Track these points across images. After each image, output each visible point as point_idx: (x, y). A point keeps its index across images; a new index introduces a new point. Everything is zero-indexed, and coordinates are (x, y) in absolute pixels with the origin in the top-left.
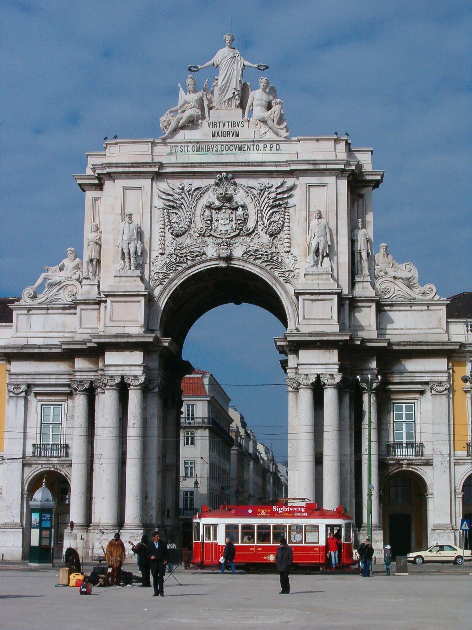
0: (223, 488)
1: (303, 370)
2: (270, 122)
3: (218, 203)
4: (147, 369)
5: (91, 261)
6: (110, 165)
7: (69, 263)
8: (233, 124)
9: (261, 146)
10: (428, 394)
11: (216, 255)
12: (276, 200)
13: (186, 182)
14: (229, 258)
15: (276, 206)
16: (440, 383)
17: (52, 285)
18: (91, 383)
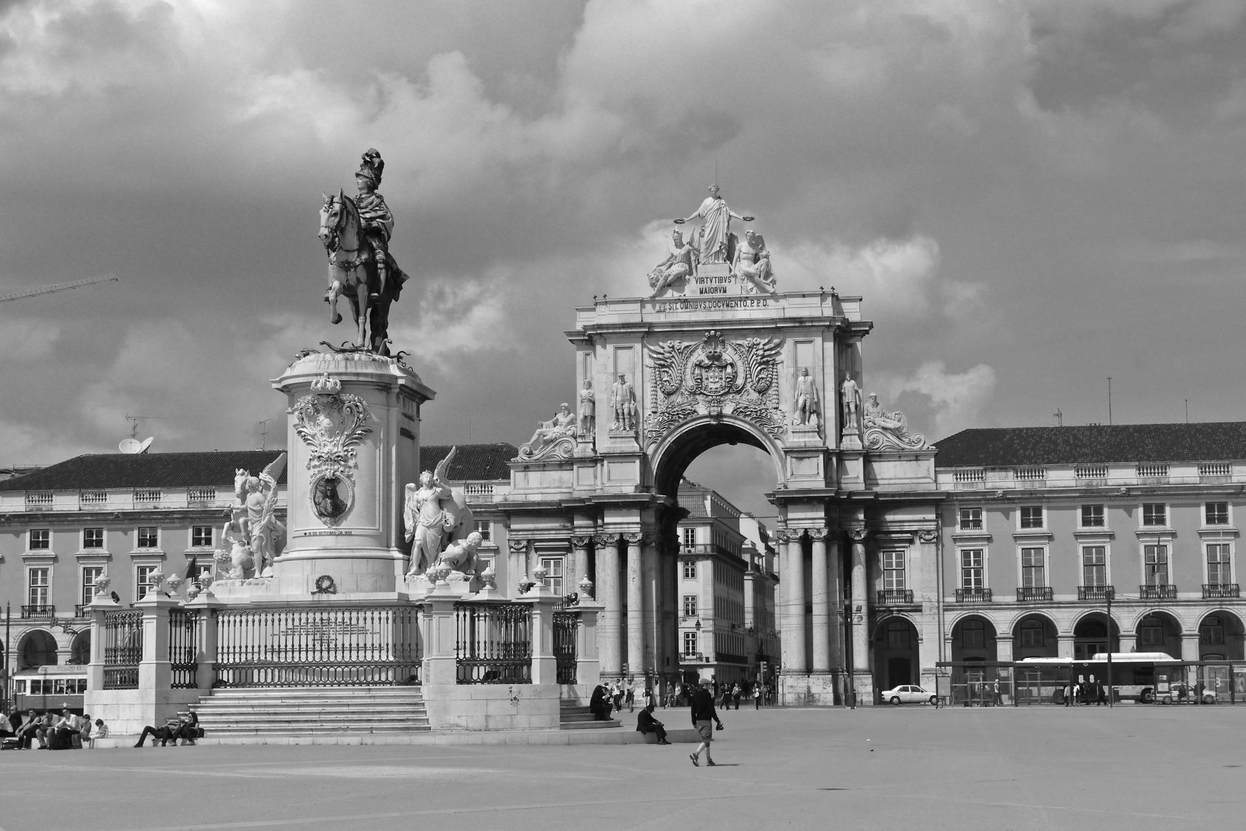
0: (733, 626)
1: (791, 525)
2: (757, 278)
3: (707, 361)
4: (643, 524)
5: (586, 417)
6: (600, 326)
7: (561, 417)
8: (721, 280)
9: (749, 302)
10: (917, 541)
11: (706, 413)
12: (763, 356)
13: (676, 343)
14: (720, 416)
15: (764, 363)
16: (929, 532)
17: (547, 443)
18: (591, 538)
